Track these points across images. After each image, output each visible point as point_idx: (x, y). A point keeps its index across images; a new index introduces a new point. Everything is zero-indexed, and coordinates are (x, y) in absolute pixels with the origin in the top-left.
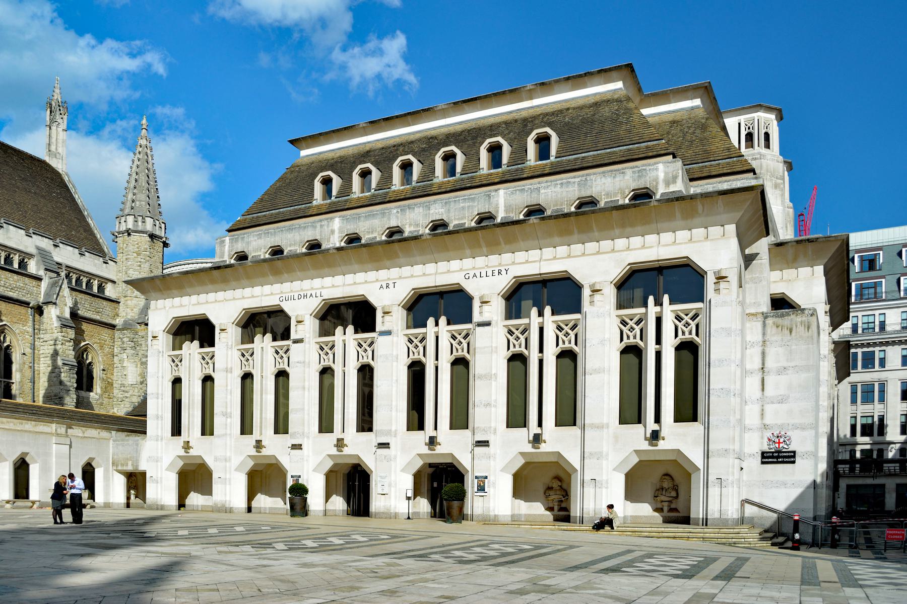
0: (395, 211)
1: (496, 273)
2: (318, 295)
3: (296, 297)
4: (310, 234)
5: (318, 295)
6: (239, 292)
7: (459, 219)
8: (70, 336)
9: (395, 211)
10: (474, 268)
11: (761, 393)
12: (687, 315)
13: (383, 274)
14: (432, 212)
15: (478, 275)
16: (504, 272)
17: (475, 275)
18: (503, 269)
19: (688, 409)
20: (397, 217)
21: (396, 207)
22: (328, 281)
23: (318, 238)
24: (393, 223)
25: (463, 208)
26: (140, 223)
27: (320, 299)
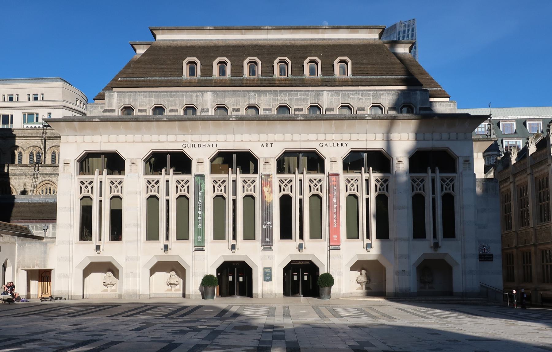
1: (340, 145)
2: (214, 145)
3: (197, 146)
4: (186, 101)
5: (214, 145)
6: (146, 138)
7: (298, 105)
9: (253, 94)
10: (325, 140)
13: (263, 137)
14: (279, 98)
16: (344, 145)
17: (326, 145)
18: (344, 143)
19: (450, 232)
20: (255, 98)
22: (222, 137)
23: (194, 103)
24: (252, 102)
25: (301, 99)
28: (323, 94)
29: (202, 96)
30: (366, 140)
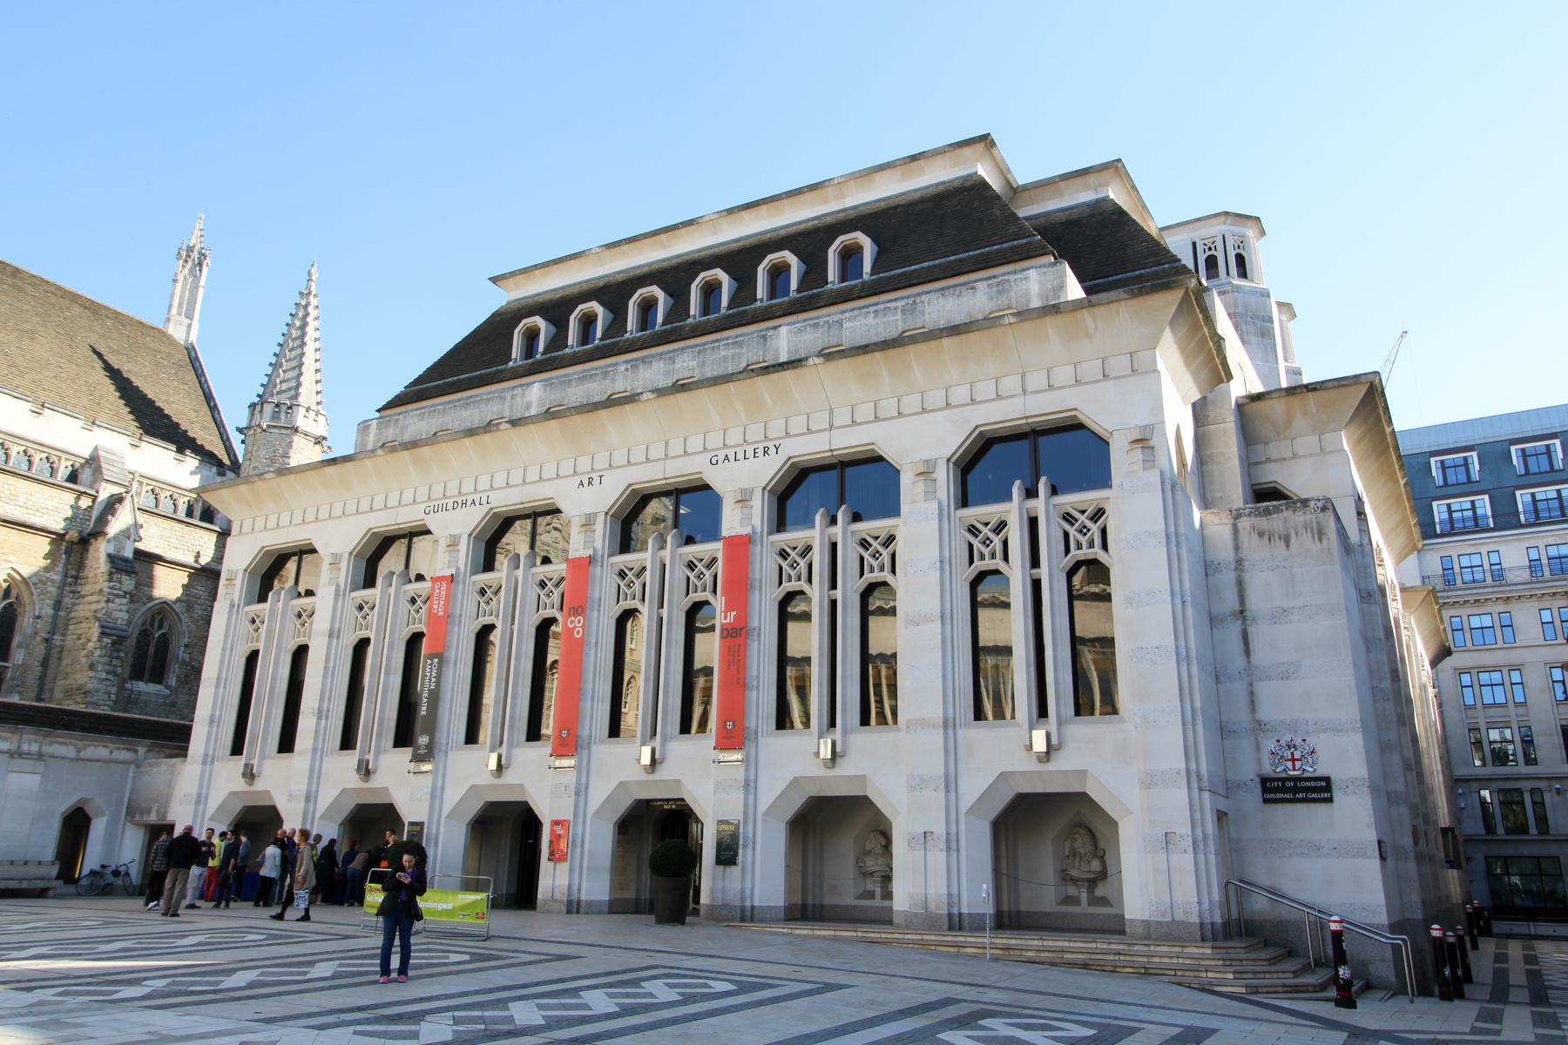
0: (622, 368)
1: (760, 452)
2: (484, 501)
3: (450, 507)
5: (484, 501)
8: (125, 588)
9: (622, 368)
11: (1244, 659)
12: (1083, 512)
14: (677, 366)
15: (732, 457)
16: (772, 450)
18: (770, 445)
20: (626, 378)
21: (626, 362)
25: (726, 358)
26: (283, 416)
27: (486, 508)
28: (778, 335)
29: (523, 396)
30: (831, 427)
